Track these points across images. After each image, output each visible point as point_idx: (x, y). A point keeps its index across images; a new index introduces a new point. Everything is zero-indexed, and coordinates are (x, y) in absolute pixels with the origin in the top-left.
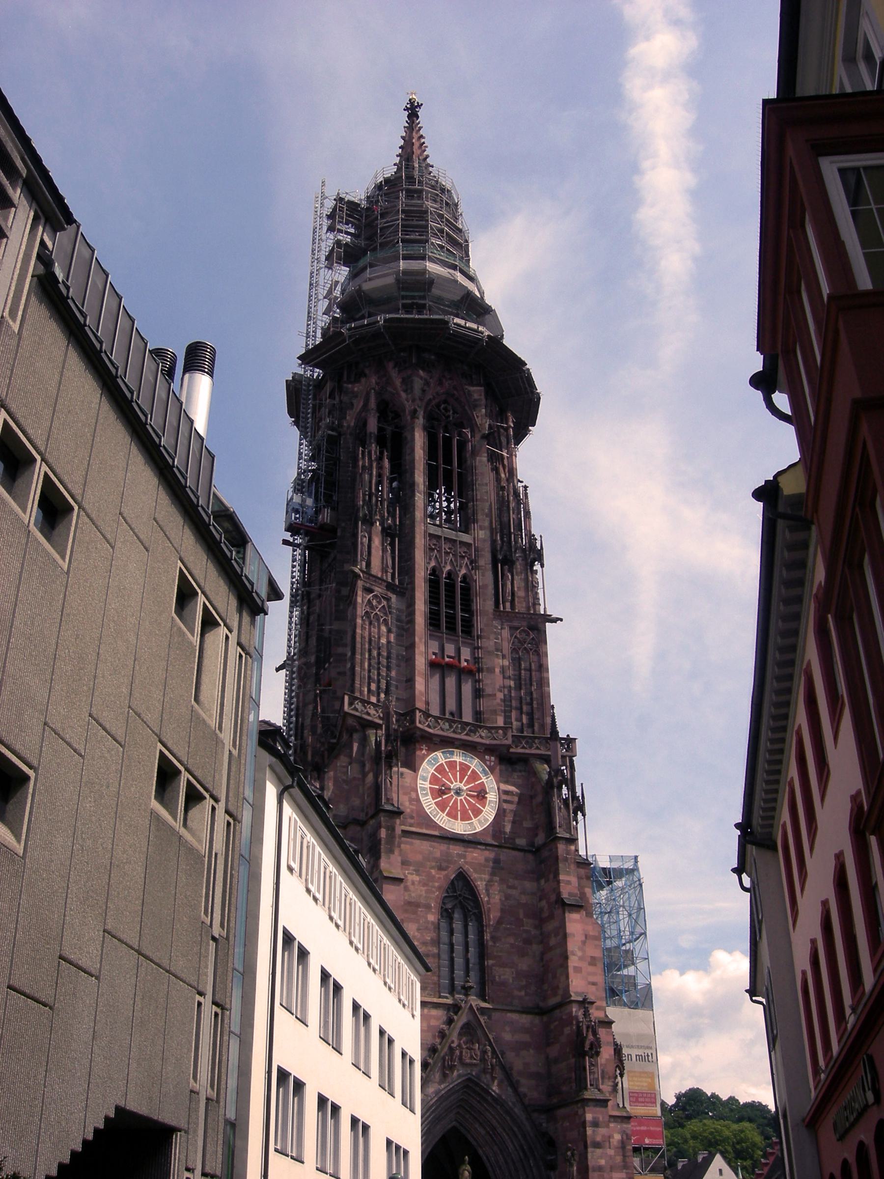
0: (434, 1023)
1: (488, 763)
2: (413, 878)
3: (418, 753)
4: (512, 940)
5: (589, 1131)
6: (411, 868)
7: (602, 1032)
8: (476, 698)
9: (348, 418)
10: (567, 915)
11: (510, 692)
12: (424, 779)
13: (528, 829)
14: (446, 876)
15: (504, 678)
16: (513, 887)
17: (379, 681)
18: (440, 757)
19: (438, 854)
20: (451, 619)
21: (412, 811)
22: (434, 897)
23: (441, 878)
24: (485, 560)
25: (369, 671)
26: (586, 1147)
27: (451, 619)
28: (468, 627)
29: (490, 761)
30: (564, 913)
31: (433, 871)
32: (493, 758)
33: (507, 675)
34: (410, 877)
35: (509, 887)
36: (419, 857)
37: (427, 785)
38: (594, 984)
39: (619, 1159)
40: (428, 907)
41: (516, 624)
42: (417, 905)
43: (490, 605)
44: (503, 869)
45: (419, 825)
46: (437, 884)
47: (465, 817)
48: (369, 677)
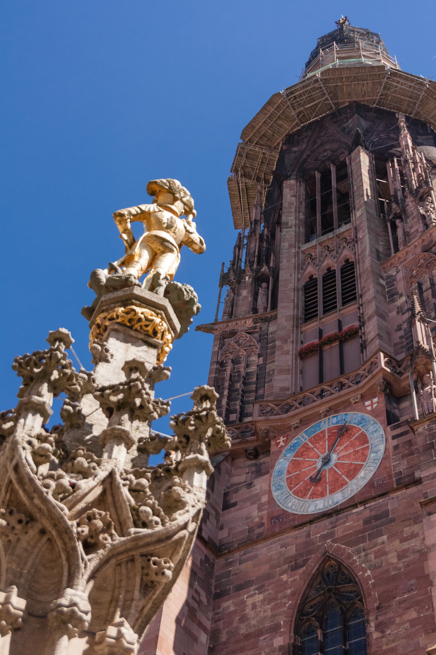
4: (413, 614)
6: (252, 588)
23: (294, 582)
34: (250, 602)
36: (264, 569)
40: (275, 629)
42: (259, 633)
44: (393, 520)
46: (289, 591)
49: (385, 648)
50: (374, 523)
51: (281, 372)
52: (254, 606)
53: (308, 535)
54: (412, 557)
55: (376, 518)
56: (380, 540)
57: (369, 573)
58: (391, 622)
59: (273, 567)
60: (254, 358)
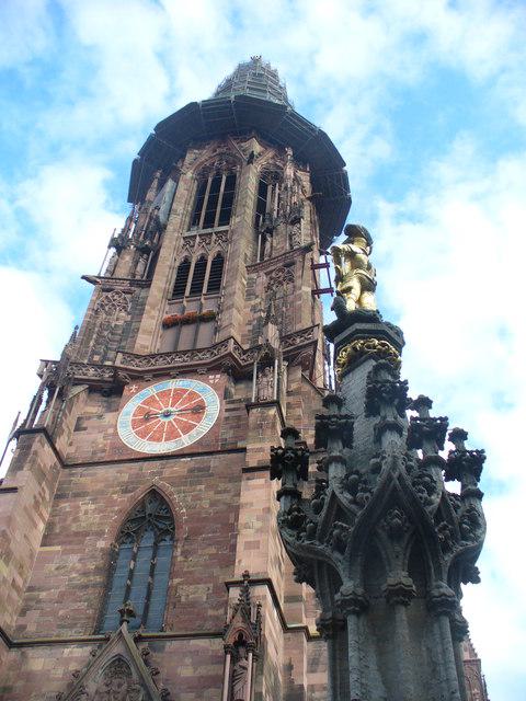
0: (73, 667)
4: (213, 550)
12: (127, 414)
16: (225, 491)
18: (152, 390)
22: (114, 520)
23: (123, 502)
28: (215, 285)
32: (218, 376)
34: (83, 508)
36: (100, 486)
37: (131, 417)
40: (100, 534)
42: (87, 534)
44: (212, 475)
46: (116, 508)
47: (172, 435)
49: (185, 570)
51: (145, 332)
52: (86, 513)
54: (221, 507)
55: (200, 470)
56: (198, 487)
58: (194, 552)
59: (108, 486)
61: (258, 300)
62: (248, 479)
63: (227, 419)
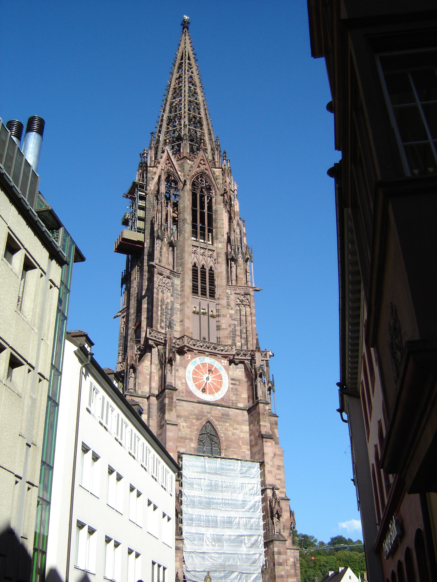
1: (223, 364)
2: (183, 424)
3: (186, 358)
5: (276, 557)
6: (182, 419)
7: (283, 504)
8: (217, 330)
9: (150, 185)
10: (264, 443)
11: (235, 327)
13: (244, 398)
14: (201, 423)
15: (232, 320)
16: (236, 429)
17: (166, 322)
19: (197, 412)
20: (204, 289)
21: (183, 389)
22: (195, 435)
23: (198, 424)
24: (222, 260)
25: (161, 316)
26: (274, 565)
27: (204, 289)
28: (212, 294)
29: (224, 363)
30: (263, 442)
31: (194, 421)
33: (234, 318)
34: (182, 424)
35: (234, 429)
36: (186, 413)
37: (191, 376)
38: (279, 479)
39: (292, 571)
40: (191, 440)
41: (238, 292)
42: (186, 439)
43: (224, 282)
44: (231, 419)
45: (187, 396)
46: (196, 428)
48: (161, 320)
50: (225, 417)
53: (202, 408)
54: (236, 437)
57: (222, 435)
60: (169, 294)
61: (232, 312)
62: (266, 442)
63: (232, 388)
